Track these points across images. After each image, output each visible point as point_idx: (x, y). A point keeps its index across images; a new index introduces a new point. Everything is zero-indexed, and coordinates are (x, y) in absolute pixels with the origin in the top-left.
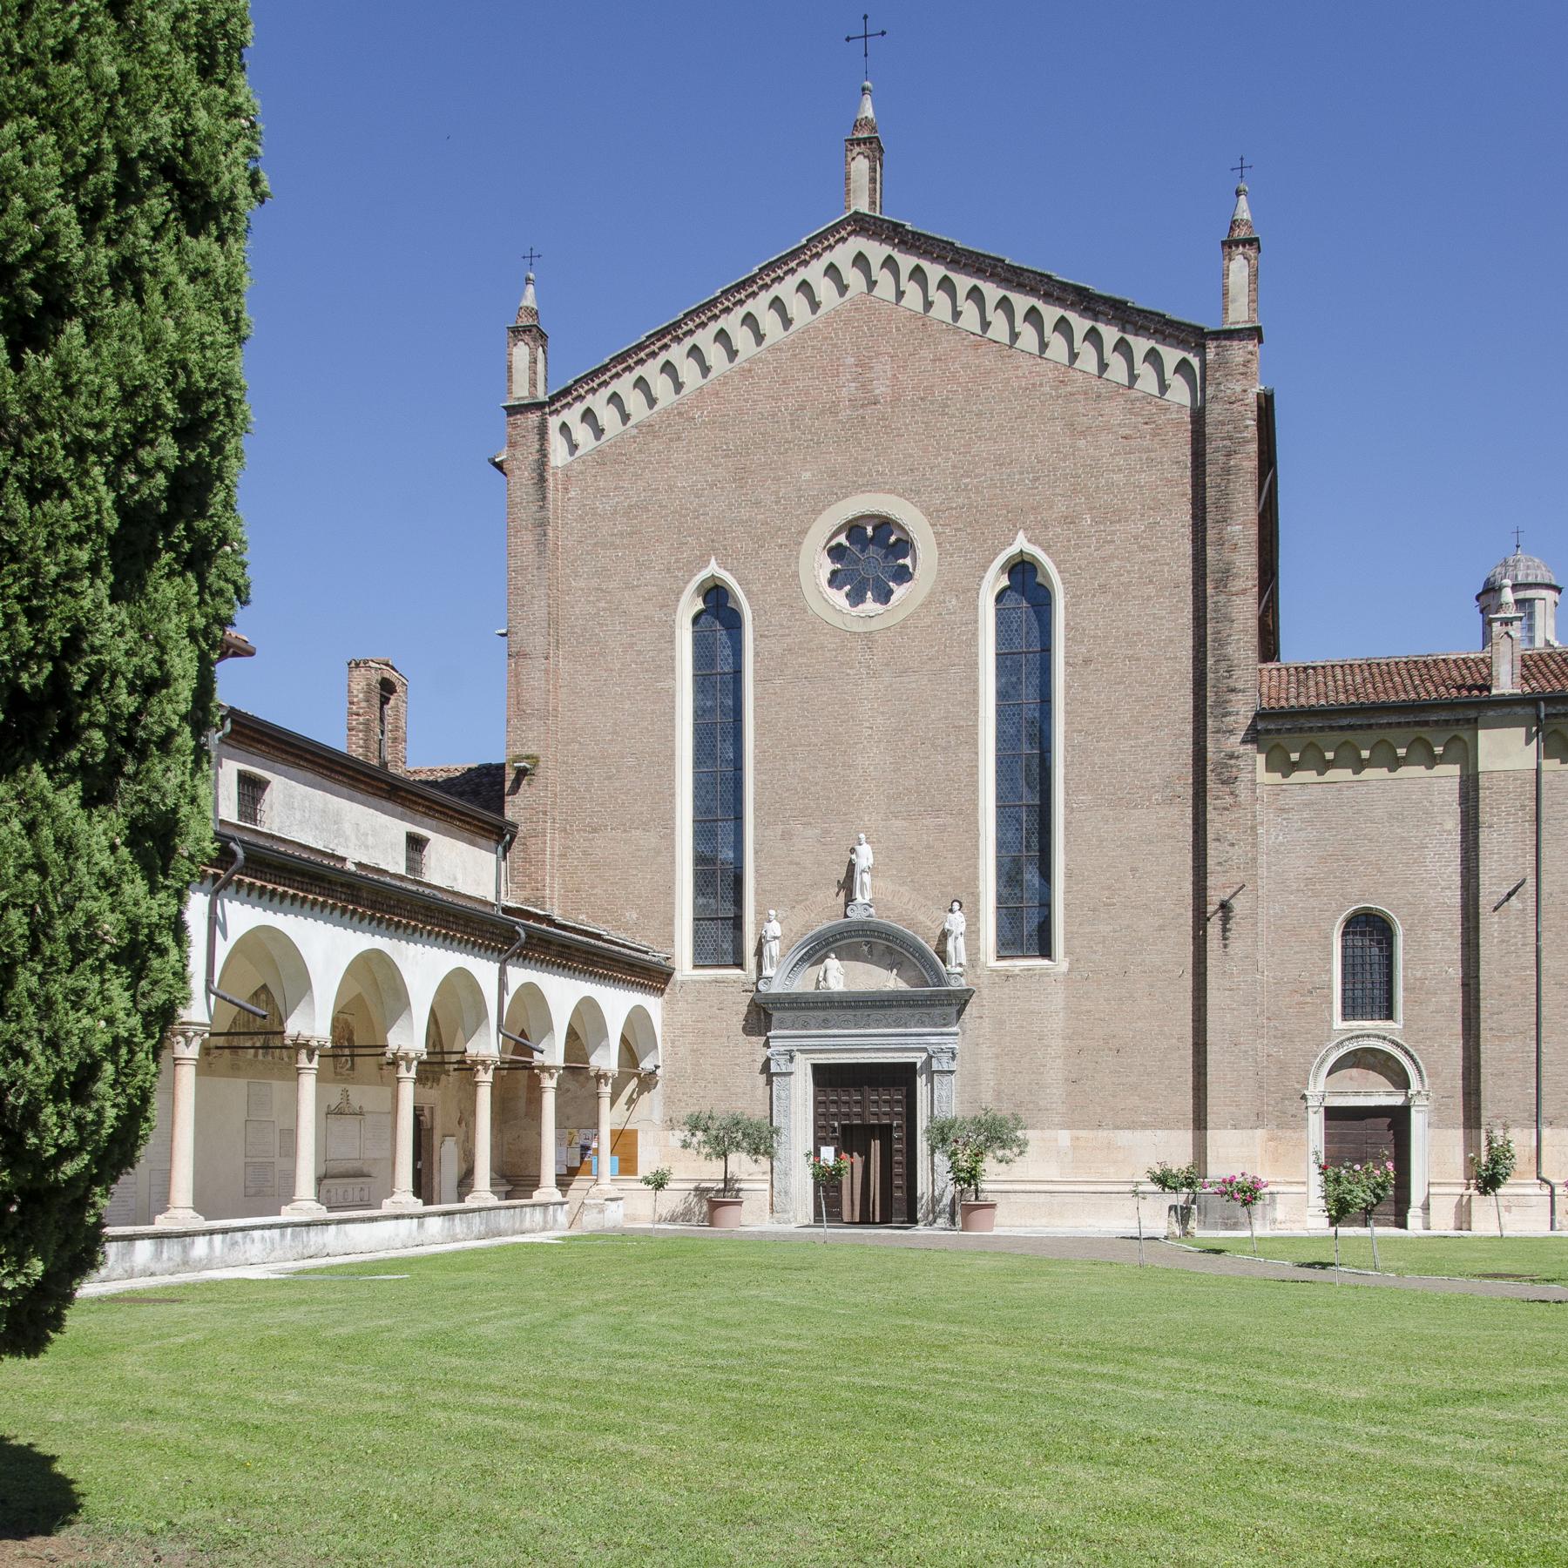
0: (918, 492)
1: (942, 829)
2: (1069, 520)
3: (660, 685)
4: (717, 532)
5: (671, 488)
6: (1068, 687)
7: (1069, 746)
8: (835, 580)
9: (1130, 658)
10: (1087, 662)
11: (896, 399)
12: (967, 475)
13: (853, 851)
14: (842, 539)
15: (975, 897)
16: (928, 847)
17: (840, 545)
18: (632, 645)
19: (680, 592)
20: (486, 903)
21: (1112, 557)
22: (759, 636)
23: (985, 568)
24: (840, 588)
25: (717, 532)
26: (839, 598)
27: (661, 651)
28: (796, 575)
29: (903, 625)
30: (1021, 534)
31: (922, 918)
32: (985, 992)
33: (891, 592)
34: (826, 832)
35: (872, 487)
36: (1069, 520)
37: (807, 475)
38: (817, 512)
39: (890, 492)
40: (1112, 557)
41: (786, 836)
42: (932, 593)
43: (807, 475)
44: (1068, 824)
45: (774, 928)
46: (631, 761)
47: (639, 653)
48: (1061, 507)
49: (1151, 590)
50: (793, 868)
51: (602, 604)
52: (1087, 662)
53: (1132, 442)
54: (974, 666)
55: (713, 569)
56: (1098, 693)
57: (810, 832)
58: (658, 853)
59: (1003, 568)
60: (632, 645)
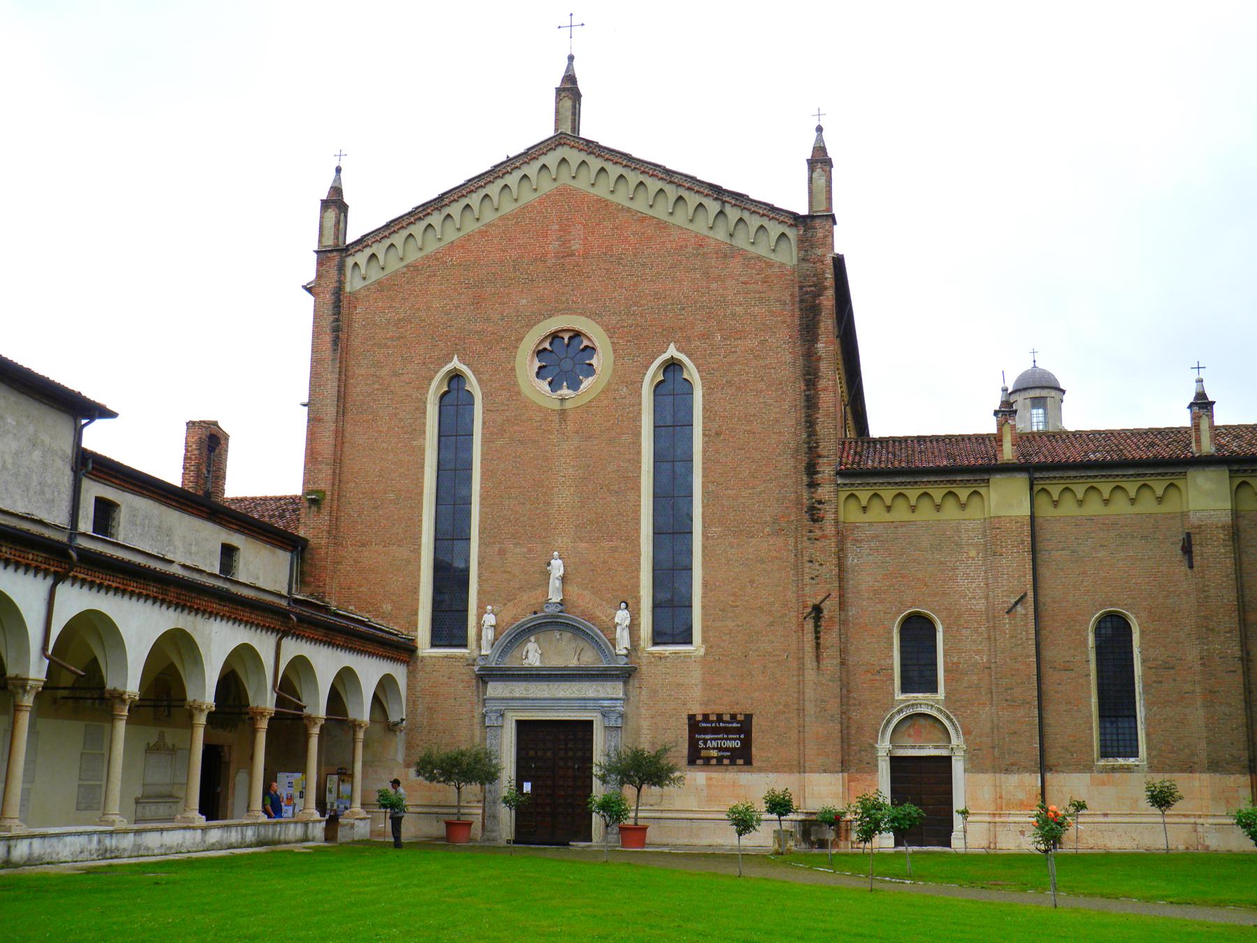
0: (600, 315)
1: (614, 550)
2: (705, 336)
3: (415, 443)
4: (459, 339)
5: (428, 308)
6: (705, 451)
7: (706, 492)
8: (540, 373)
9: (749, 432)
10: (718, 434)
11: (585, 255)
12: (635, 304)
13: (549, 564)
14: (547, 345)
15: (638, 600)
16: (604, 562)
17: (545, 349)
18: (396, 415)
19: (431, 379)
20: (281, 596)
21: (735, 362)
22: (486, 411)
23: (647, 368)
24: (544, 379)
25: (459, 339)
26: (544, 386)
27: (416, 419)
28: (513, 369)
29: (589, 405)
30: (672, 345)
31: (598, 614)
32: (644, 669)
33: (581, 382)
34: (530, 550)
35: (569, 311)
36: (705, 336)
37: (524, 301)
38: (530, 326)
39: (581, 314)
40: (735, 362)
41: (502, 552)
42: (609, 383)
43: (524, 301)
44: (704, 548)
45: (490, 619)
46: (392, 496)
47: (401, 420)
48: (700, 328)
49: (762, 386)
50: (506, 576)
51: (376, 386)
52: (718, 434)
53: (751, 287)
54: (637, 434)
55: (455, 363)
56: (726, 456)
57: (518, 550)
58: (408, 562)
59: (659, 367)
60: (396, 415)
